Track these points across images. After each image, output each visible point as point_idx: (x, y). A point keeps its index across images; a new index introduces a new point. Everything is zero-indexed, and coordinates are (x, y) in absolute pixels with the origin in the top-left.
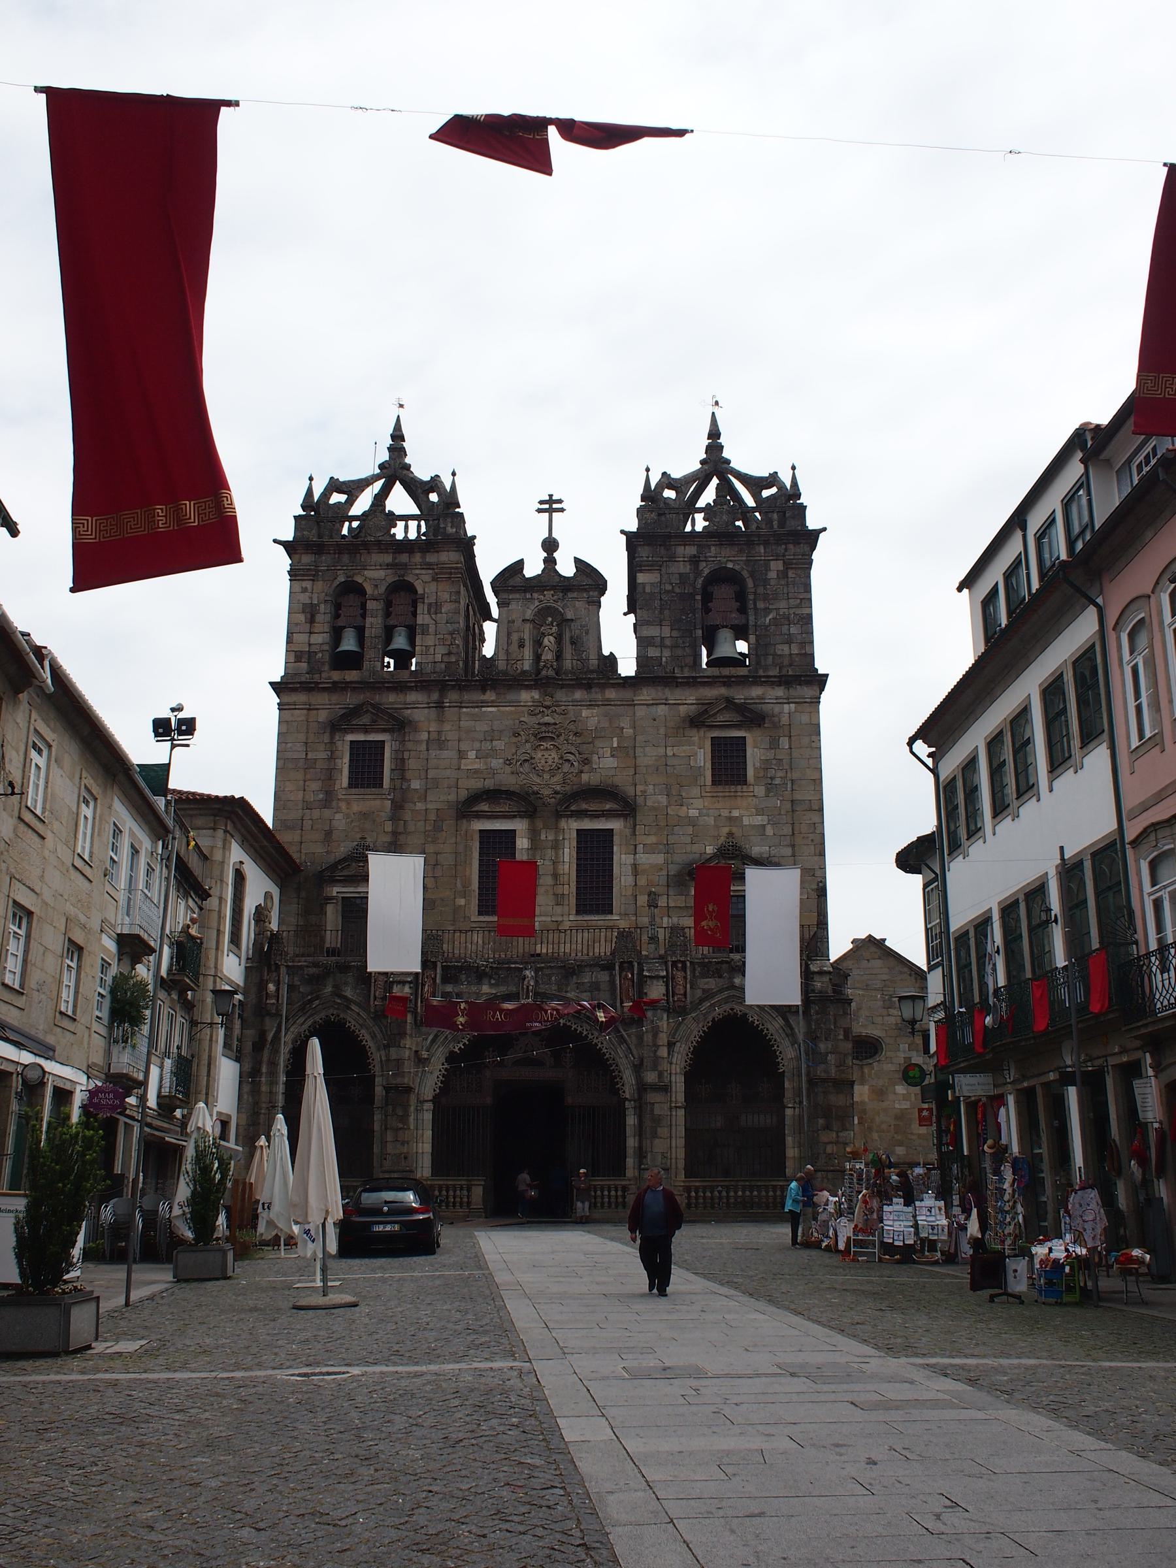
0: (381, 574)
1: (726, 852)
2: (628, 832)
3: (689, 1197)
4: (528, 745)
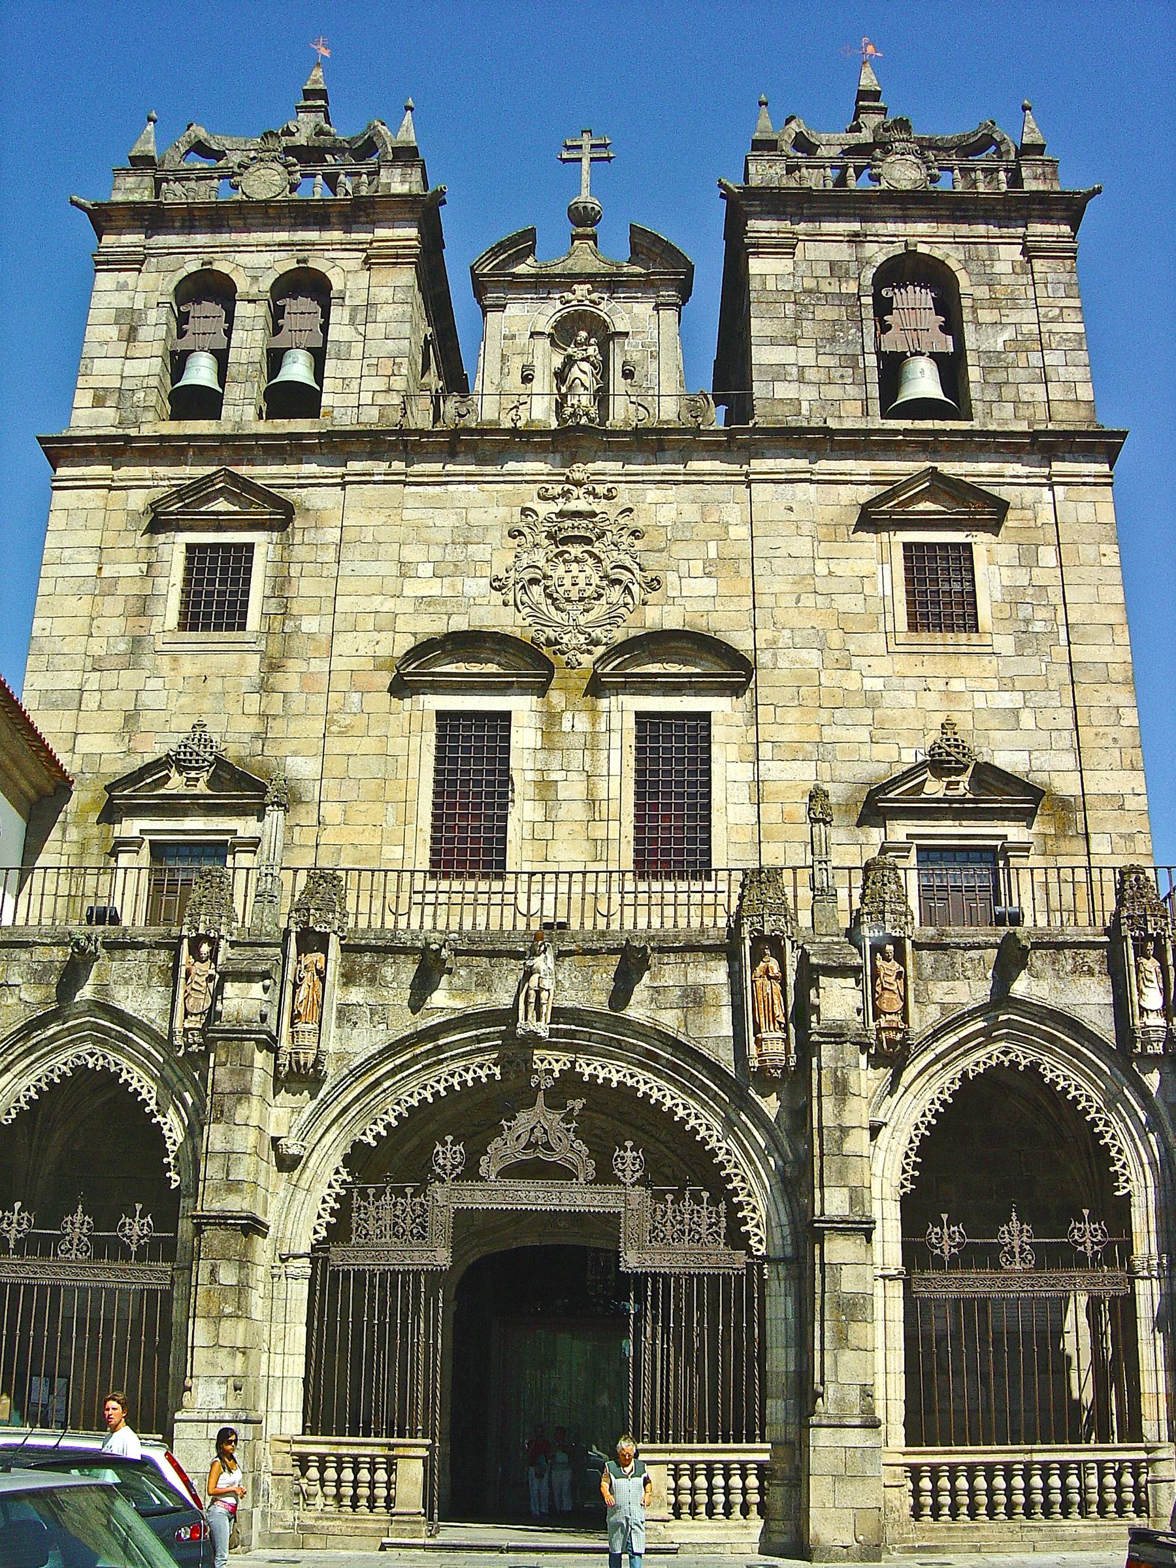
1: (944, 757)
2: (739, 718)
3: (916, 1492)
4: (539, 557)
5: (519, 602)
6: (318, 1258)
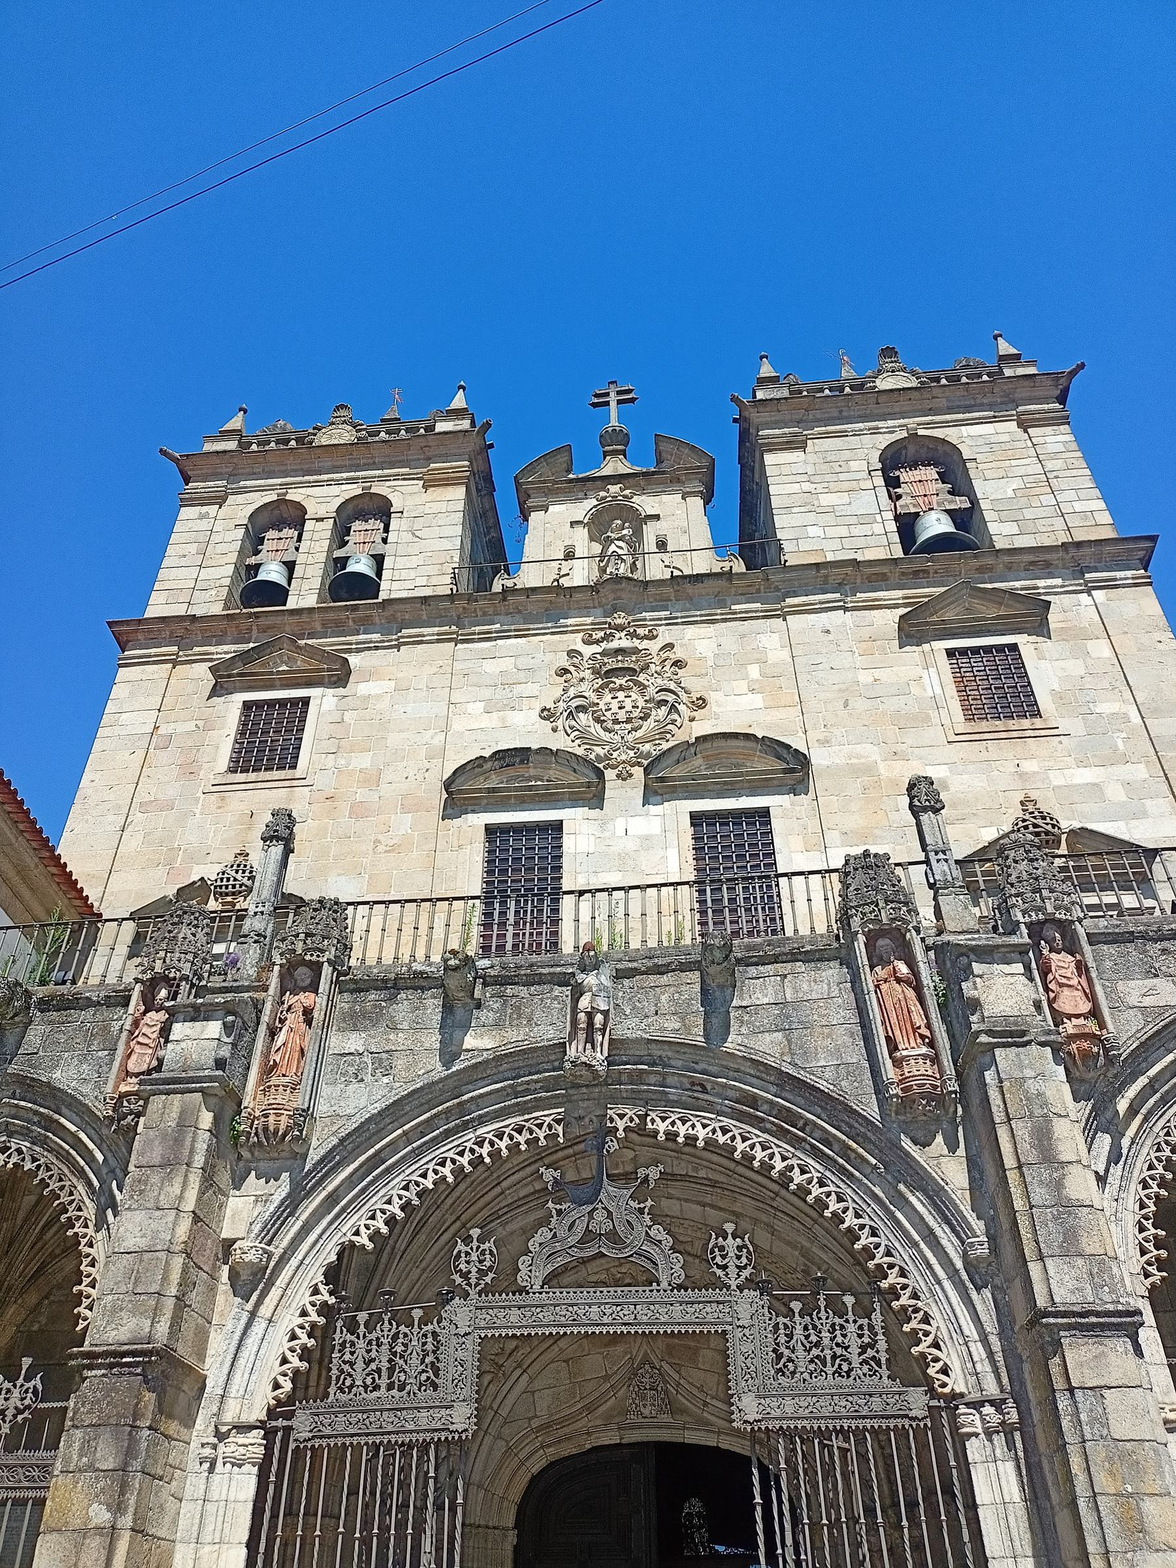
0: (335, 490)
4: (584, 687)
5: (568, 728)
6: (275, 1430)
